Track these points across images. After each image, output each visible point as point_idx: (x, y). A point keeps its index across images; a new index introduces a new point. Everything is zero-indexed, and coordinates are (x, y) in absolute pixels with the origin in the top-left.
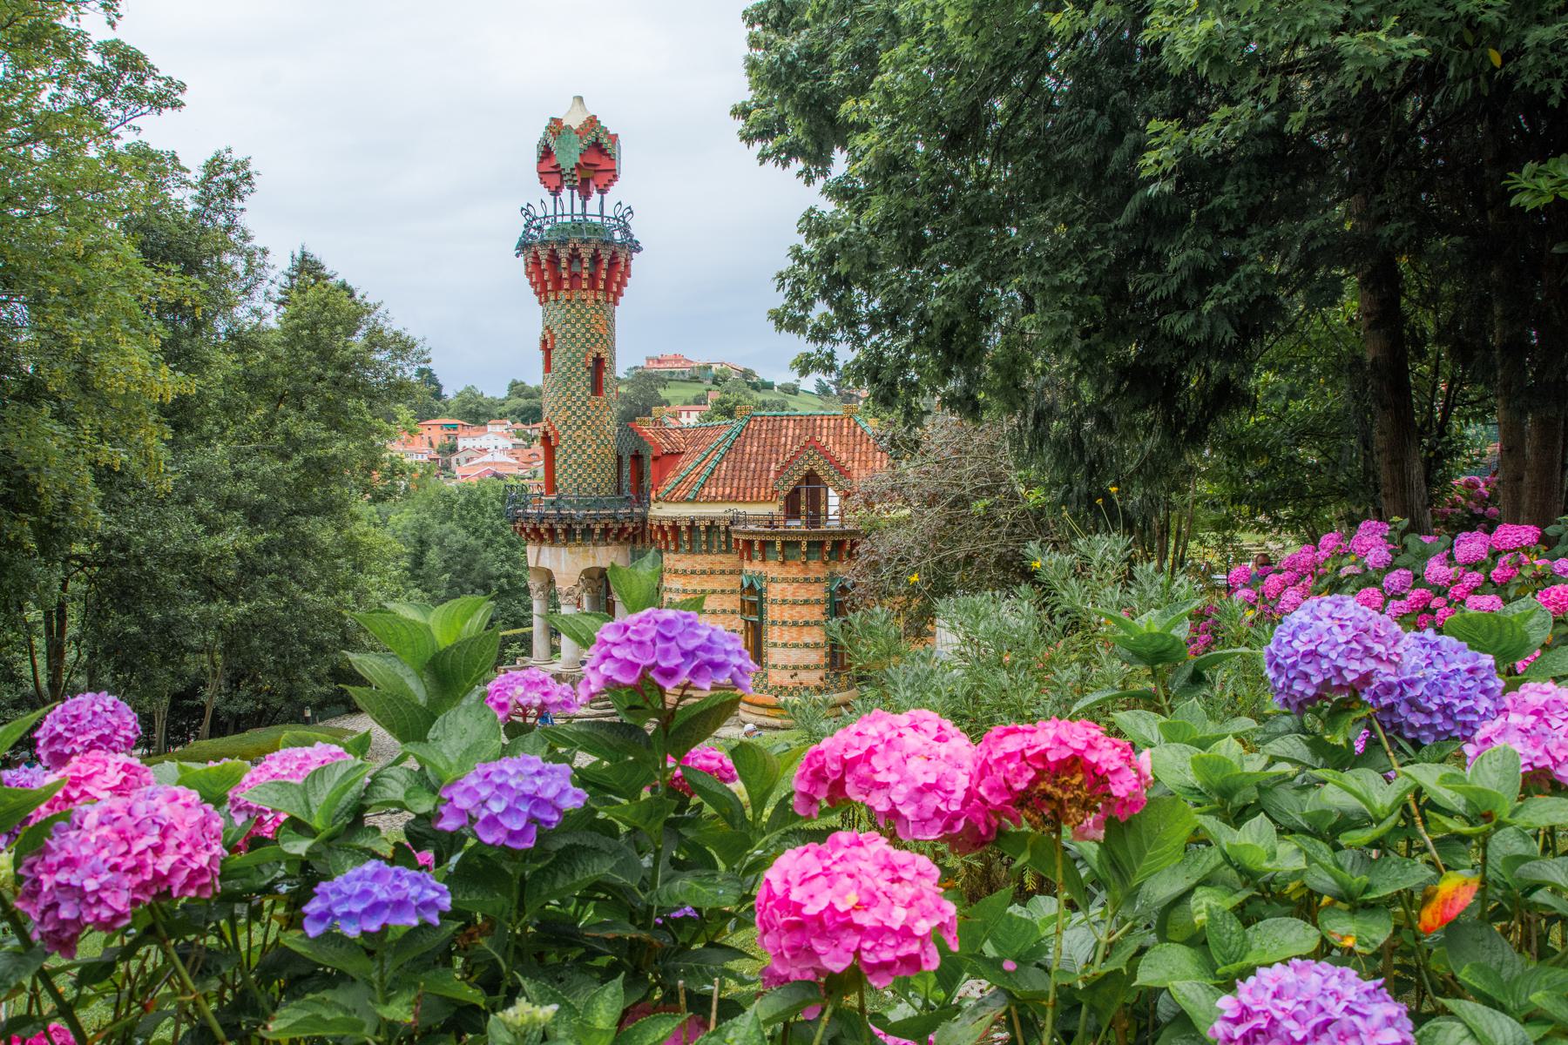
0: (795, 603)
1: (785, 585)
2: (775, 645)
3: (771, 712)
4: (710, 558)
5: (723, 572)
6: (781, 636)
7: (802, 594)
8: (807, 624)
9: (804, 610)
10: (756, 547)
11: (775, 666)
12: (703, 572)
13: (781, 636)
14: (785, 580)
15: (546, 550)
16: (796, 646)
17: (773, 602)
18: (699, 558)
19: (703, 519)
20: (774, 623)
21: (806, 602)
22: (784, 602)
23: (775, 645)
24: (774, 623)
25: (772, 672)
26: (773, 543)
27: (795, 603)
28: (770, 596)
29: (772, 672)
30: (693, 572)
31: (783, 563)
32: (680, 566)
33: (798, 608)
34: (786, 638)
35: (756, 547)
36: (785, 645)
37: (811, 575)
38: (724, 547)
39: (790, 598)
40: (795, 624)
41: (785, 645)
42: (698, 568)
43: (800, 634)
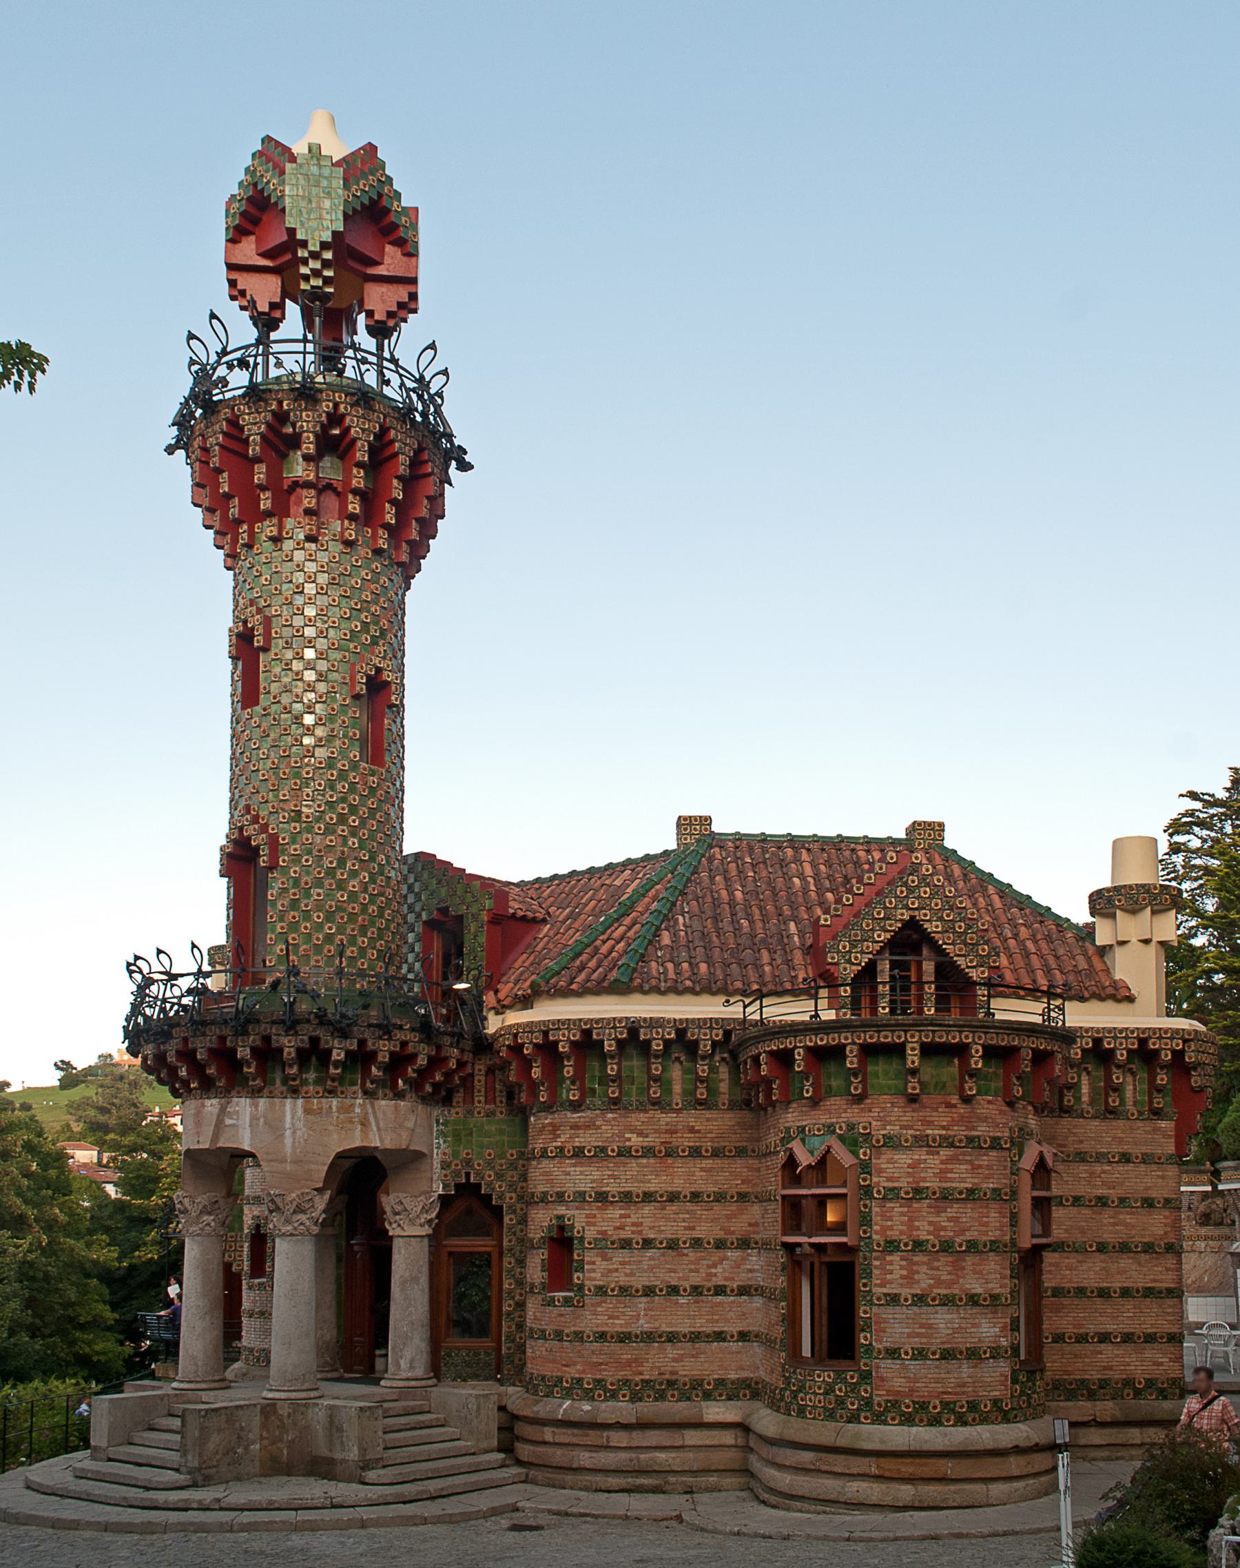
0: (945, 1197)
1: (920, 1154)
2: (894, 1299)
3: (889, 1465)
4: (665, 1119)
5: (695, 1153)
6: (909, 1279)
7: (962, 1177)
8: (972, 1246)
9: (967, 1214)
10: (852, 1062)
11: (893, 1353)
12: (648, 1152)
13: (909, 1279)
14: (921, 1141)
15: (243, 1107)
16: (948, 1301)
17: (892, 1194)
18: (638, 1119)
19: (654, 1023)
20: (891, 1246)
21: (971, 1195)
22: (918, 1193)
23: (894, 1299)
24: (891, 1246)
25: (887, 1367)
26: (898, 1051)
27: (945, 1197)
28: (880, 1182)
29: (887, 1367)
30: (624, 1153)
31: (913, 1099)
32: (586, 1139)
33: (953, 1210)
34: (924, 1281)
35: (852, 1062)
36: (920, 1300)
37: (982, 1130)
38: (702, 1093)
39: (932, 1184)
40: (946, 1247)
41: (920, 1300)
42: (635, 1140)
43: (958, 1268)
